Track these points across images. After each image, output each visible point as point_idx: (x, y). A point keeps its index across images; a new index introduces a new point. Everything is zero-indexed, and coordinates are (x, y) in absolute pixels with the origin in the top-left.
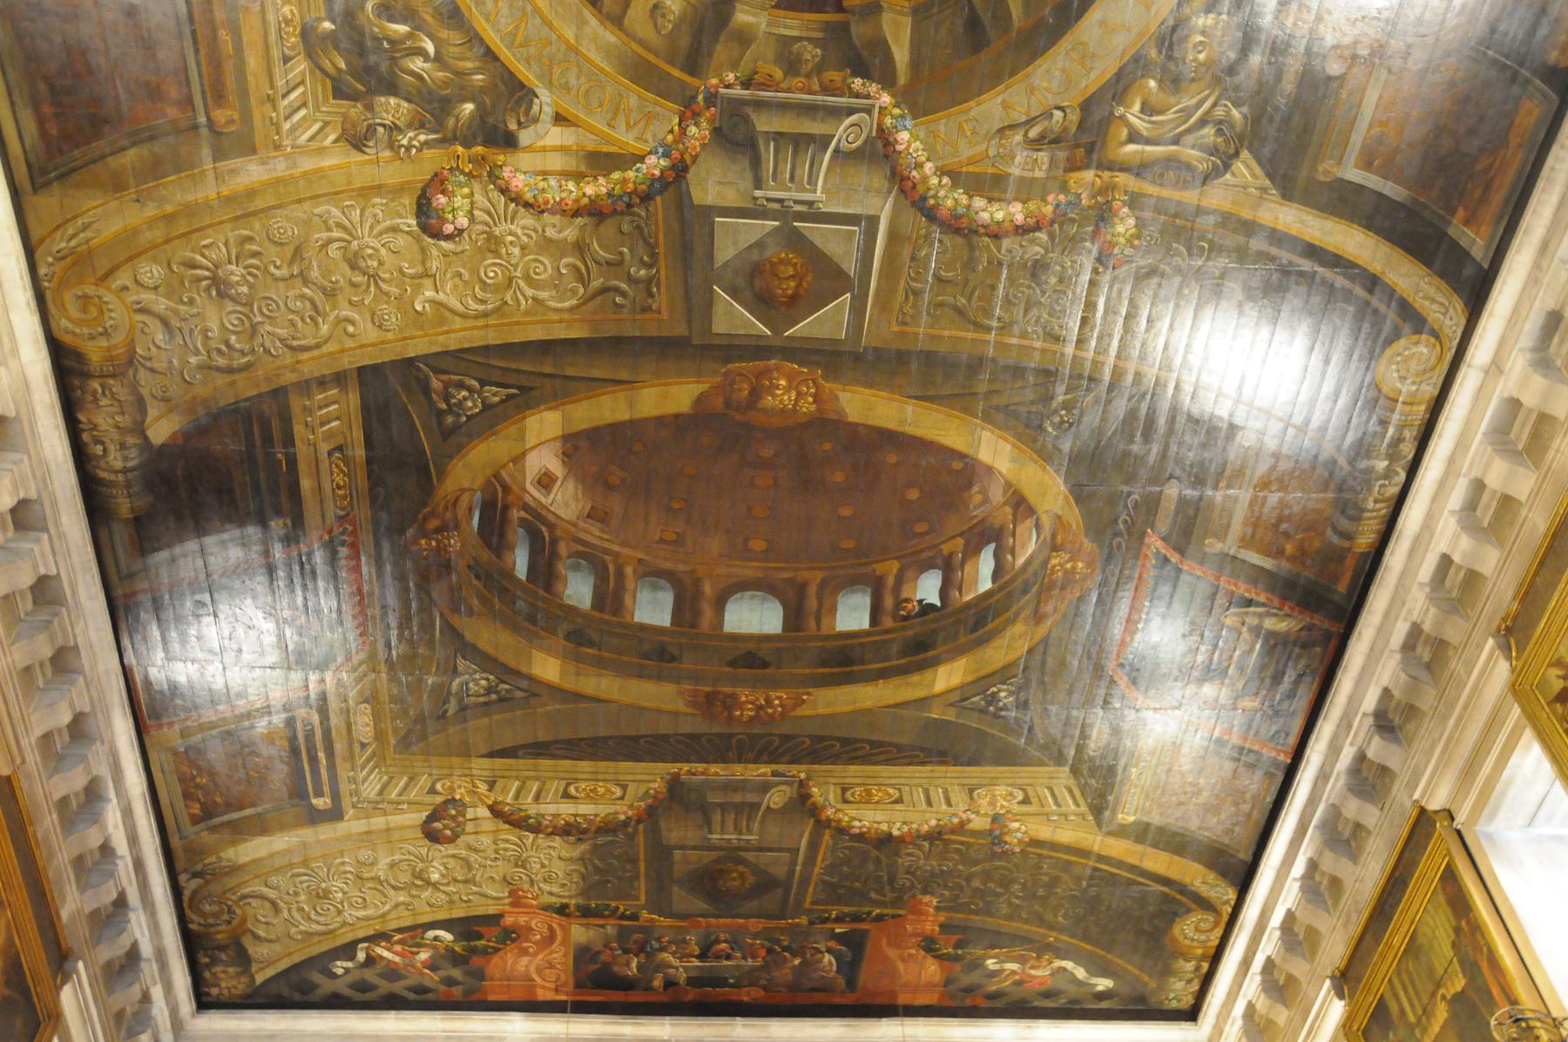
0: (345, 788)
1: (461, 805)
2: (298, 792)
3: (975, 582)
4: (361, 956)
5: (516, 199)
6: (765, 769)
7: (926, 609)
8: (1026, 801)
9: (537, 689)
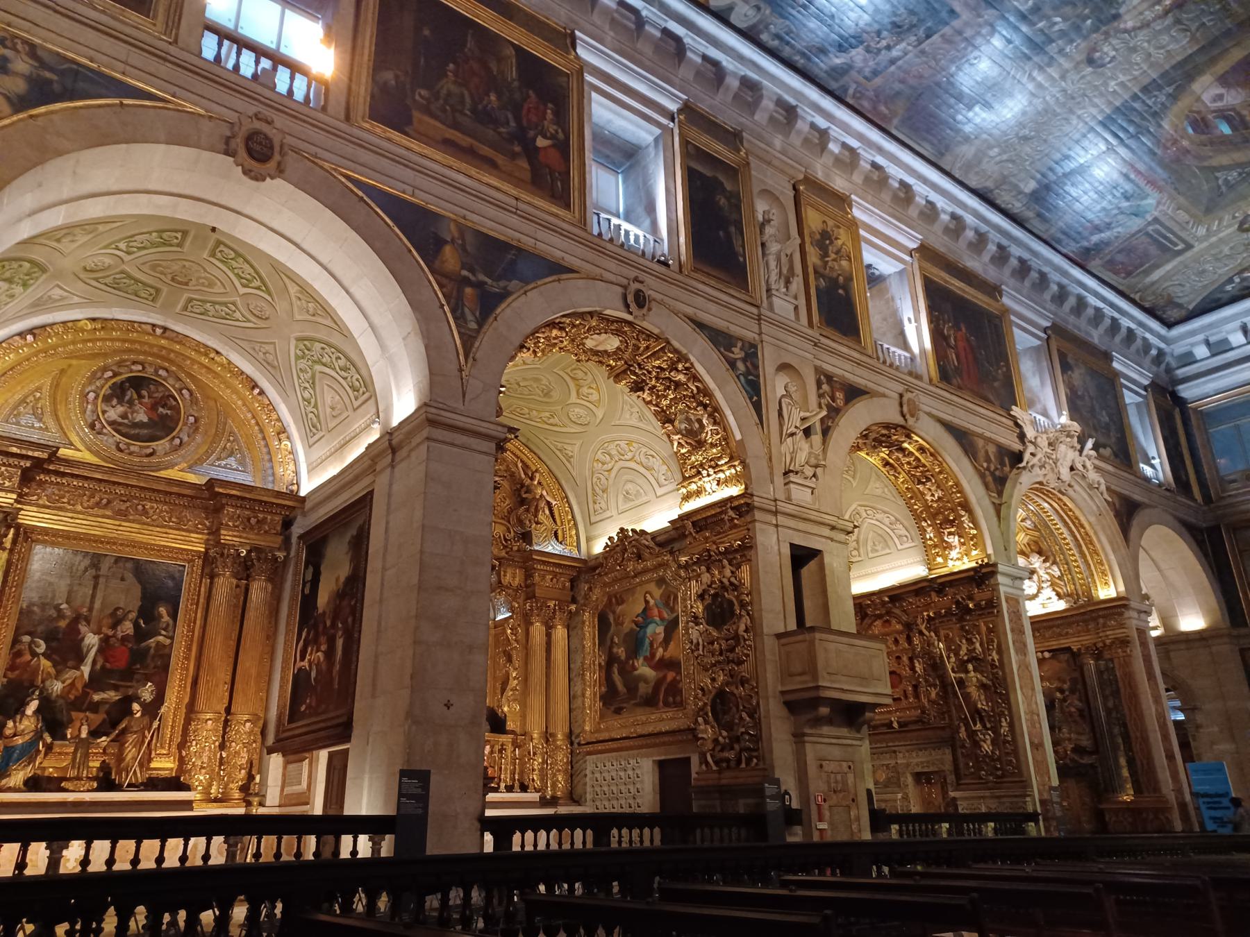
0: (1189, 239)
2: (1164, 249)
4: (1237, 280)
5: (1134, 29)
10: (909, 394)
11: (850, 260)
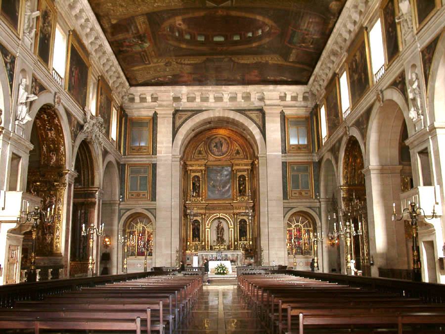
1: (171, 63)
3: (258, 33)
6: (223, 57)
7: (250, 37)
8: (272, 59)
9: (182, 49)
10: (59, 94)
11: (51, 27)
